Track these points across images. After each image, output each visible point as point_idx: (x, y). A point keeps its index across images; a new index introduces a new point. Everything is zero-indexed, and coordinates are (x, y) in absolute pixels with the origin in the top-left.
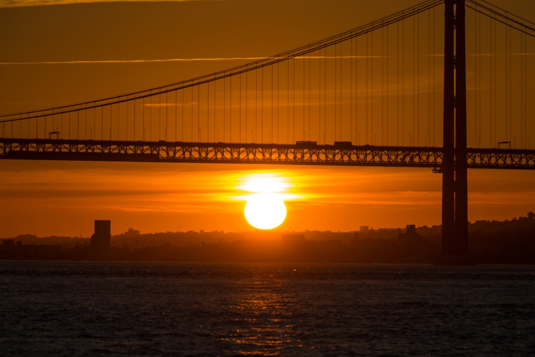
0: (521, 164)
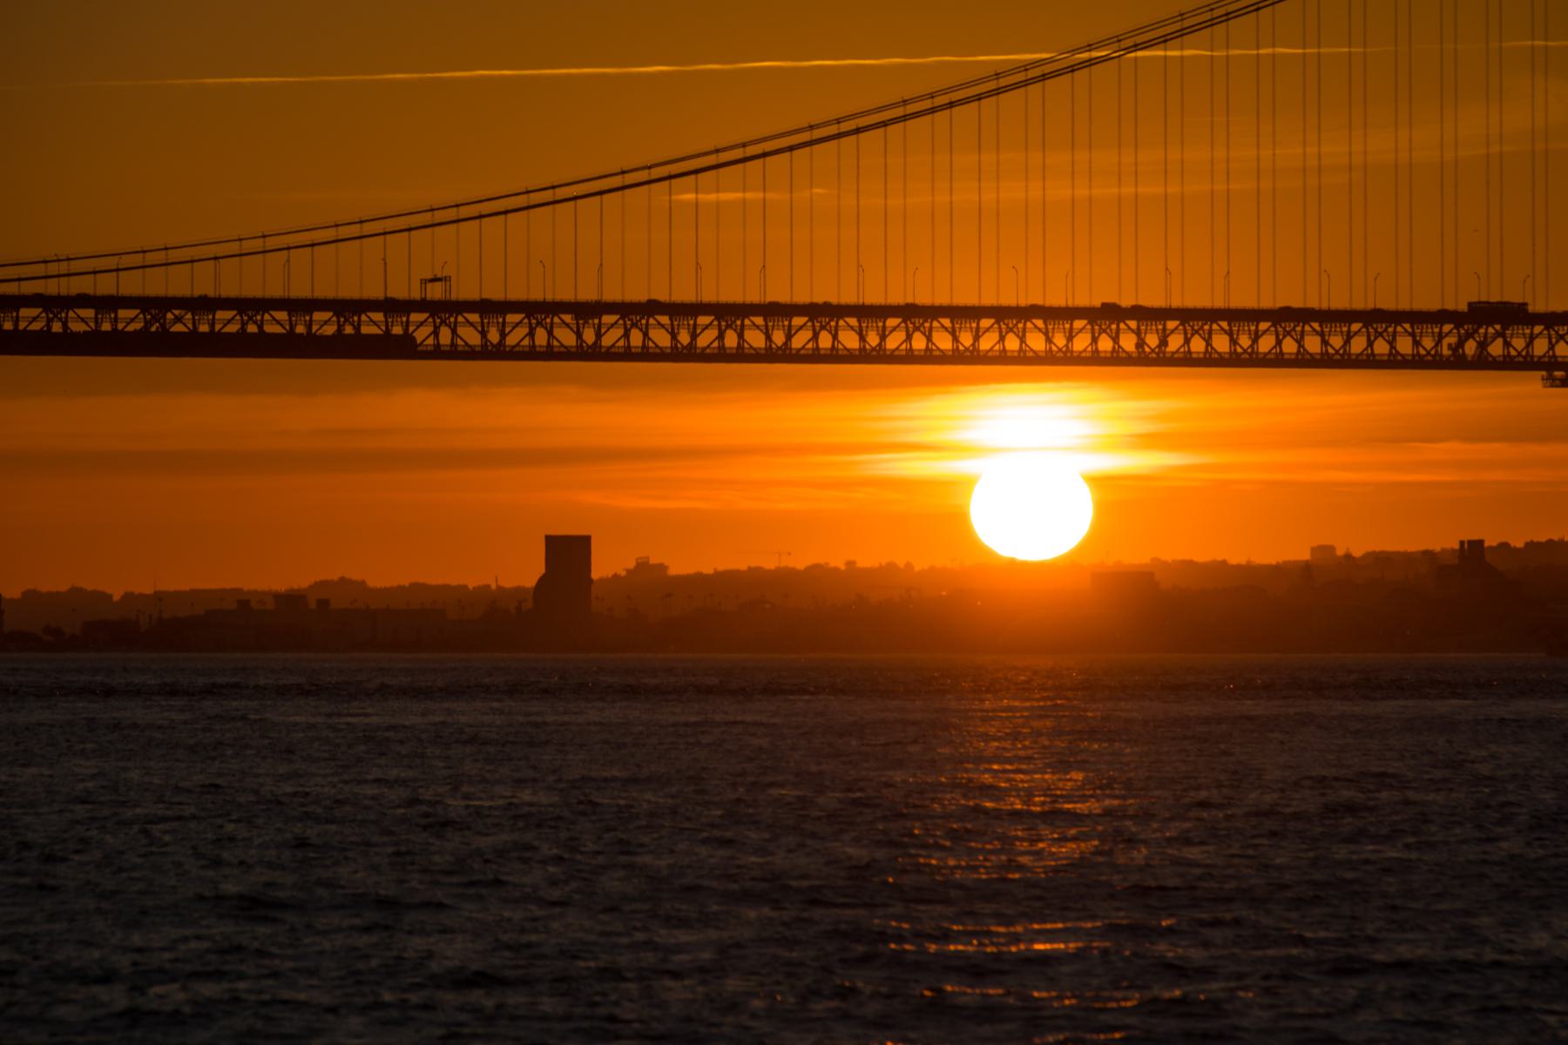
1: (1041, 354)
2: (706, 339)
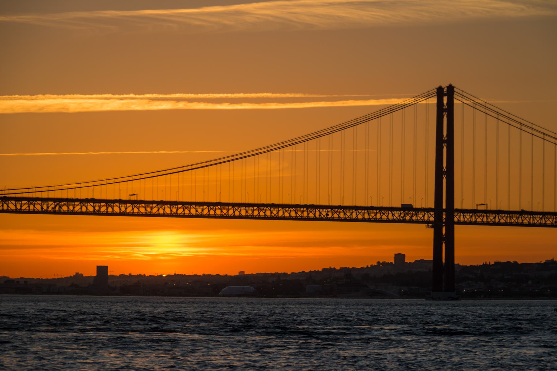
0: (424, 219)
2: (103, 209)
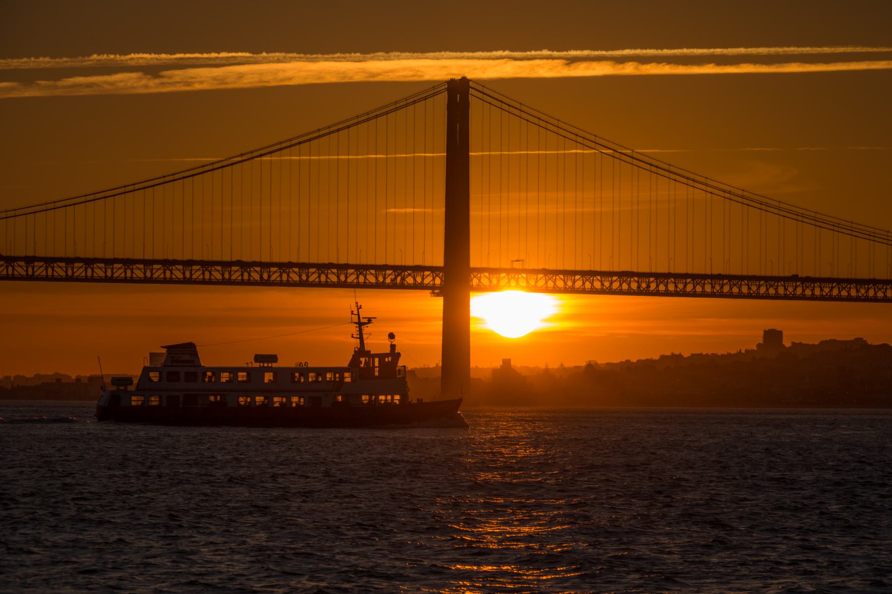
1: (672, 292)
